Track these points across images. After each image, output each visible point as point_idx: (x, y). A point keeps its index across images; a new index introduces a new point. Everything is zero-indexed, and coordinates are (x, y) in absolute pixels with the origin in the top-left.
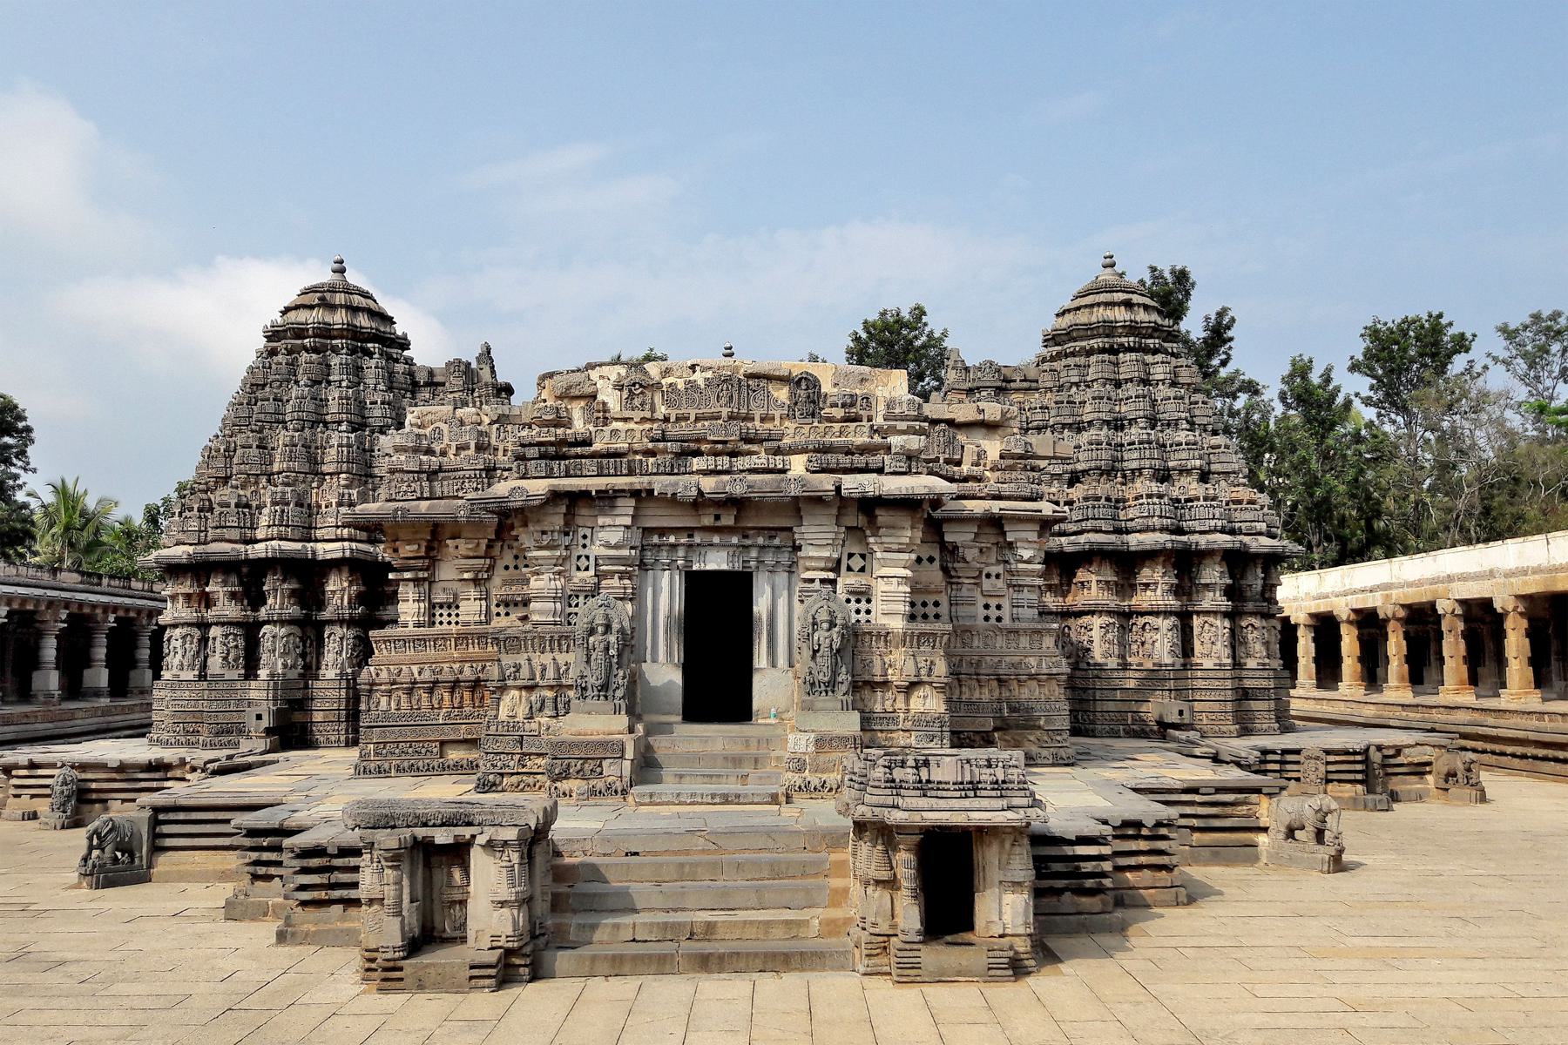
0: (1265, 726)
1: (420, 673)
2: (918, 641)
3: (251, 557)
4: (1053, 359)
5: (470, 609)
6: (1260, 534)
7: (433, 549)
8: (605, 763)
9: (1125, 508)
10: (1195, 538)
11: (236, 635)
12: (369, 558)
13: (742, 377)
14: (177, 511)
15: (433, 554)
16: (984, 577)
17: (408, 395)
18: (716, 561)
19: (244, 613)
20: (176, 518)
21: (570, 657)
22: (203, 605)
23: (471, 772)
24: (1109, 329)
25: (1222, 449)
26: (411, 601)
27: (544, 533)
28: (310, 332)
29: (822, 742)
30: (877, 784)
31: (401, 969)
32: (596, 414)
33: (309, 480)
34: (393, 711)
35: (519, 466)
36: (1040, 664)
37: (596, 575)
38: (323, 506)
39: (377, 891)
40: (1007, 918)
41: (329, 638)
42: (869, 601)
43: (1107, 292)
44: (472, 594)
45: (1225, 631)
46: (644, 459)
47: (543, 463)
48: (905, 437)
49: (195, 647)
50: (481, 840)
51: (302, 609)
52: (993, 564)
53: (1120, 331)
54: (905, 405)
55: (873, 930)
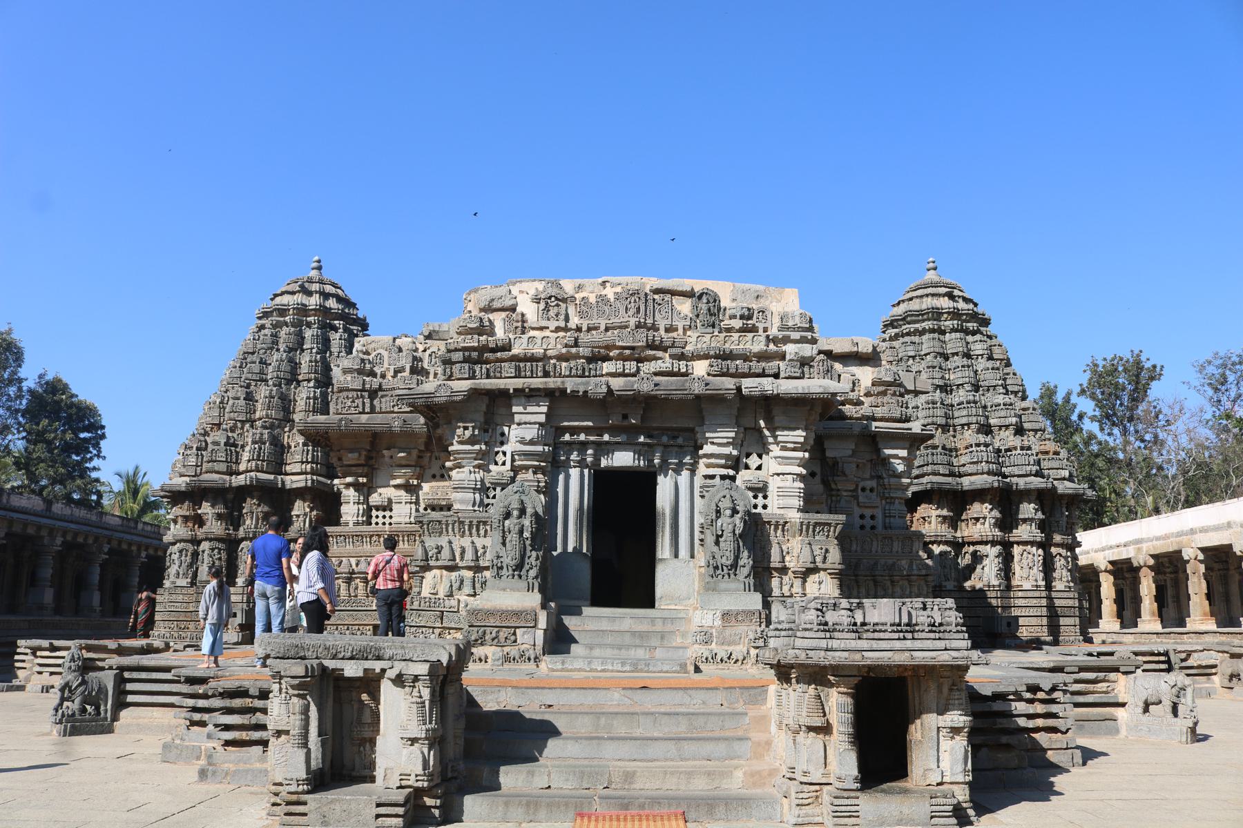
0: (1071, 638)
1: (357, 565)
2: (814, 531)
3: (234, 485)
4: (891, 339)
5: (403, 513)
6: (1064, 479)
7: (371, 458)
8: (517, 630)
9: (957, 456)
10: (1015, 480)
12: (326, 490)
13: (648, 292)
15: (372, 462)
16: (860, 488)
18: (623, 459)
21: (488, 542)
22: (196, 526)
24: (936, 314)
25: (1031, 411)
26: (352, 503)
27: (466, 428)
29: (726, 615)
30: (808, 626)
31: (305, 803)
32: (515, 324)
35: (445, 370)
36: (911, 565)
37: (512, 470)
39: (284, 722)
40: (945, 764)
42: (765, 497)
43: (932, 287)
45: (1040, 558)
46: (558, 363)
47: (466, 366)
48: (797, 345)
49: (189, 559)
50: (391, 674)
52: (867, 479)
53: (945, 316)
54: (797, 320)
55: (805, 780)
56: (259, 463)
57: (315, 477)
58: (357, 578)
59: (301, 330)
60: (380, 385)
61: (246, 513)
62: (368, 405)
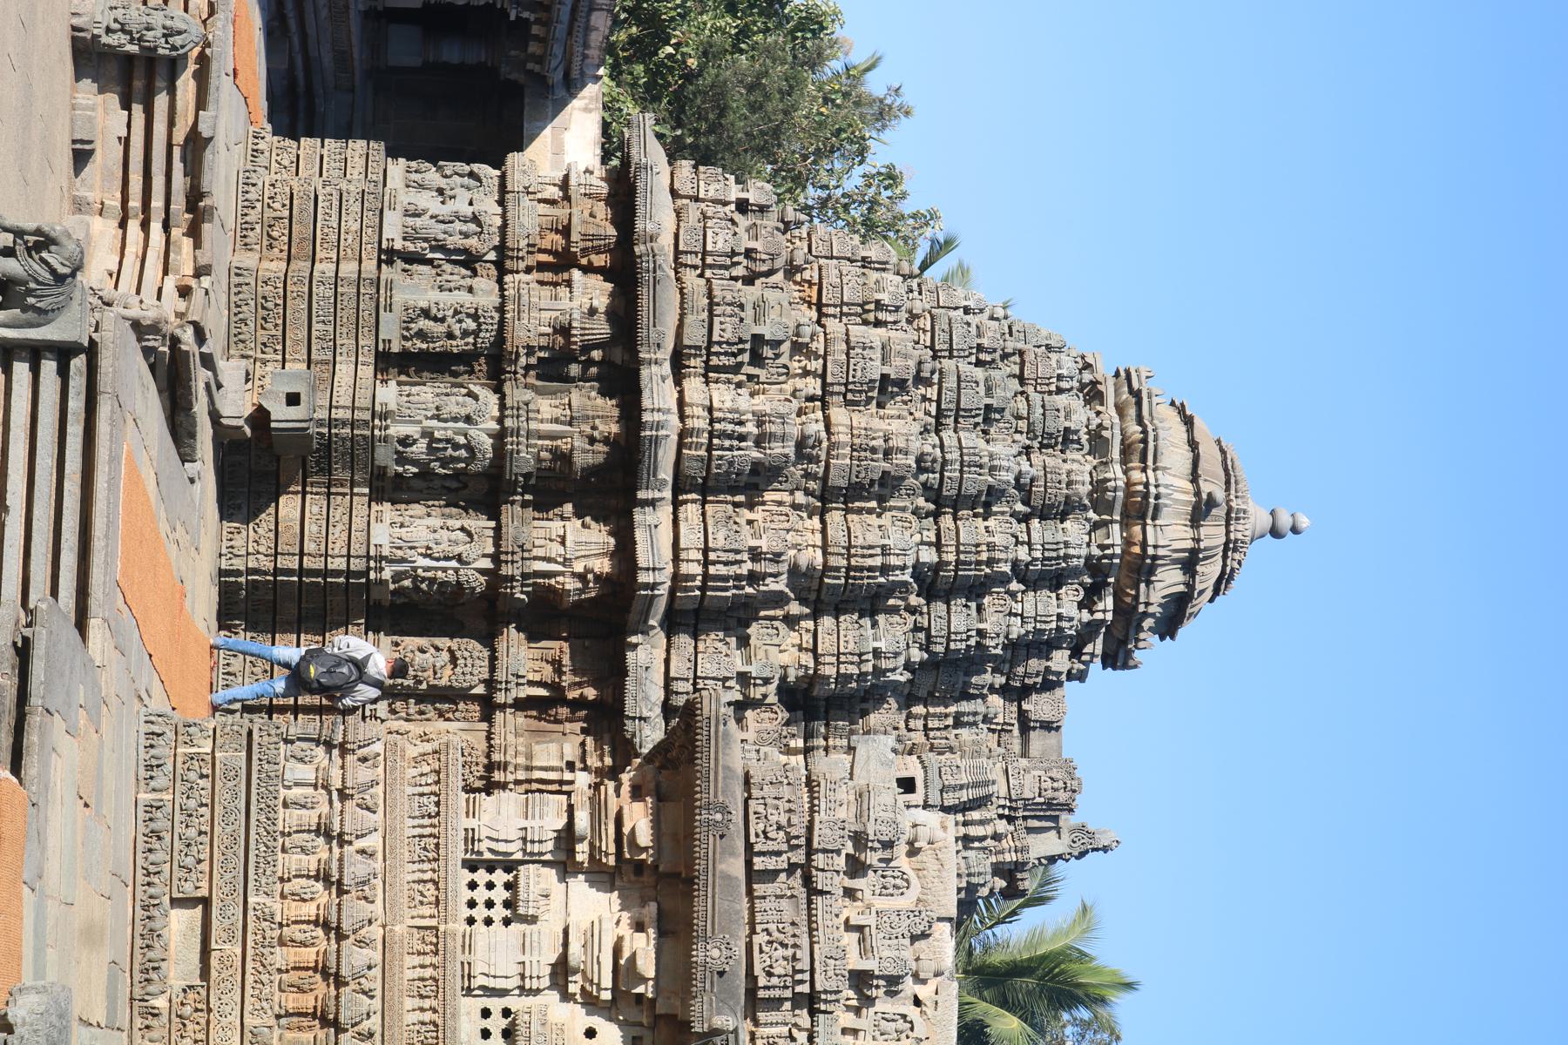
1: (362, 852)
3: (645, 372)
11: (476, 333)
12: (633, 617)
14: (753, 197)
17: (1000, 680)
19: (522, 351)
20: (734, 193)
23: (136, 967)
26: (524, 824)
28: (1137, 476)
33: (812, 485)
34: (283, 792)
38: (751, 516)
41: (462, 529)
49: (455, 241)
51: (527, 476)
56: (704, 439)
57: (663, 591)
58: (330, 849)
59: (1085, 508)
60: (822, 893)
62: (770, 863)
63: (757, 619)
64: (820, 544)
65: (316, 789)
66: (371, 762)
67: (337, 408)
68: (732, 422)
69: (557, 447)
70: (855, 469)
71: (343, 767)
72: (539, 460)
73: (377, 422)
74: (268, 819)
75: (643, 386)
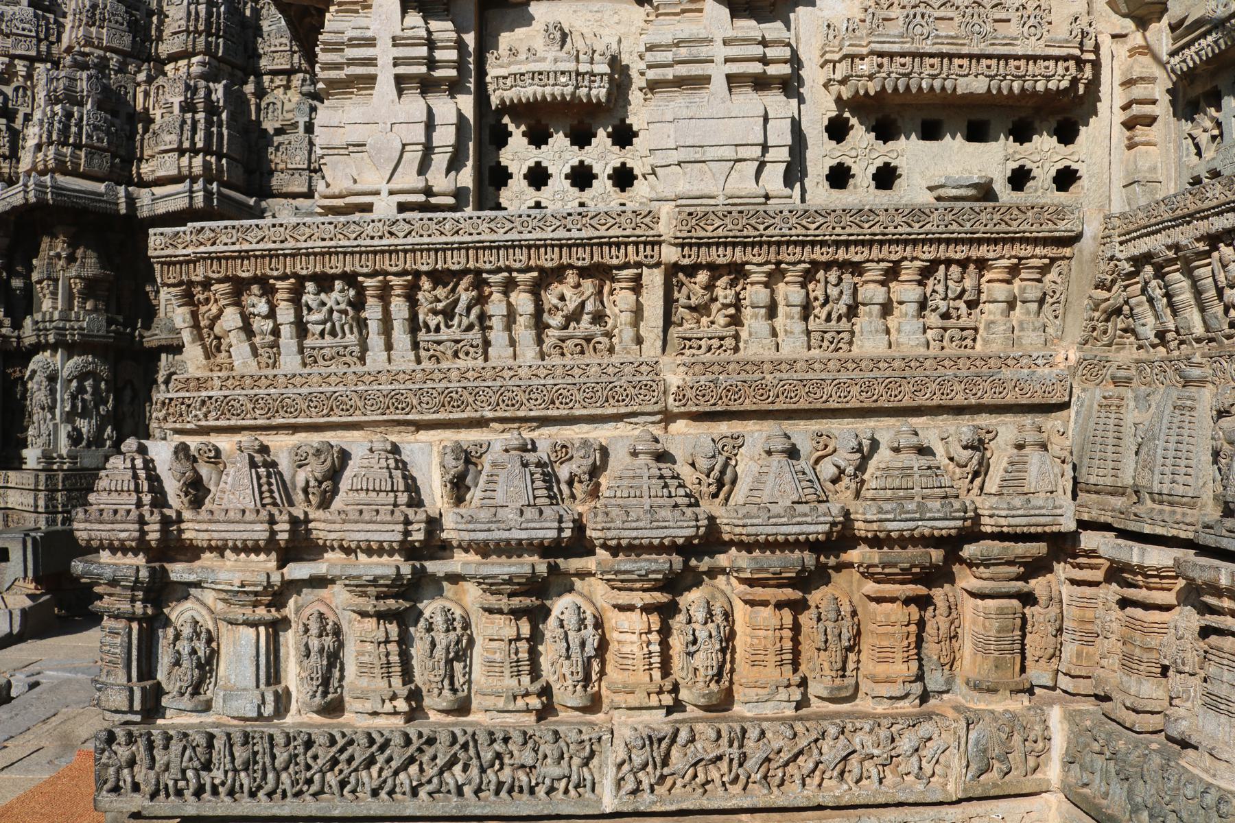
1: (458, 487)
44: (720, 52)
51: (109, 322)
56: (67, 150)
58: (455, 578)
61: (40, 282)
63: (259, 122)
64: (186, 61)
65: (277, 627)
66: (204, 470)
67: (36, 507)
68: (51, 124)
69: (79, 292)
70: (112, 24)
71: (220, 550)
72: (95, 310)
73: (55, 467)
74: (370, 761)
75: (8, 208)
